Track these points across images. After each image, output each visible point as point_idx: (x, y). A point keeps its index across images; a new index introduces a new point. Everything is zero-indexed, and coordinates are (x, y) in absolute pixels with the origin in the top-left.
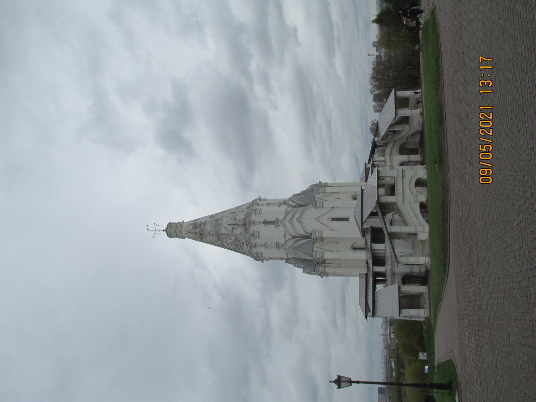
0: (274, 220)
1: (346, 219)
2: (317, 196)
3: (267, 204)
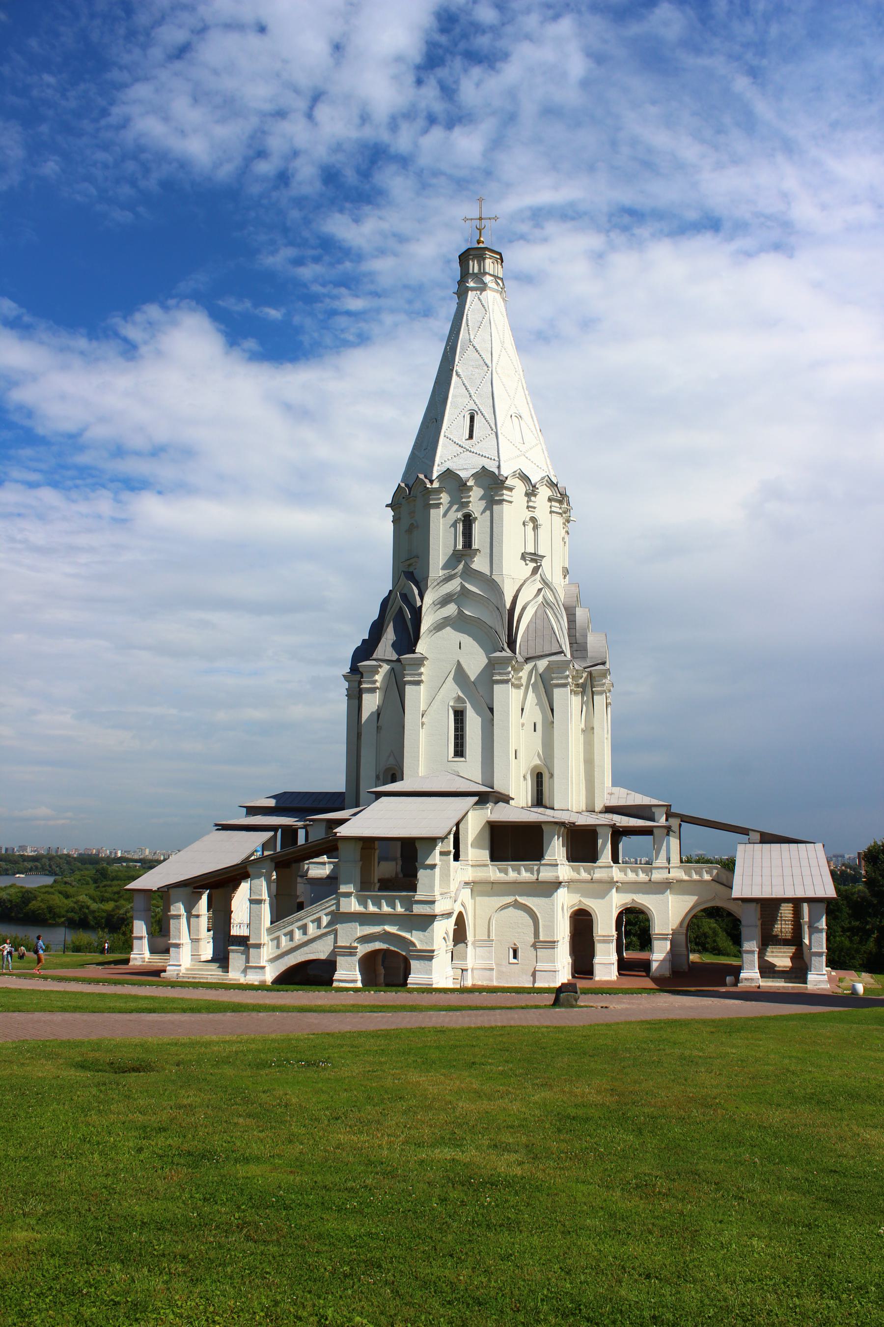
0: (475, 546)
1: (459, 751)
2: (542, 664)
3: (533, 520)
